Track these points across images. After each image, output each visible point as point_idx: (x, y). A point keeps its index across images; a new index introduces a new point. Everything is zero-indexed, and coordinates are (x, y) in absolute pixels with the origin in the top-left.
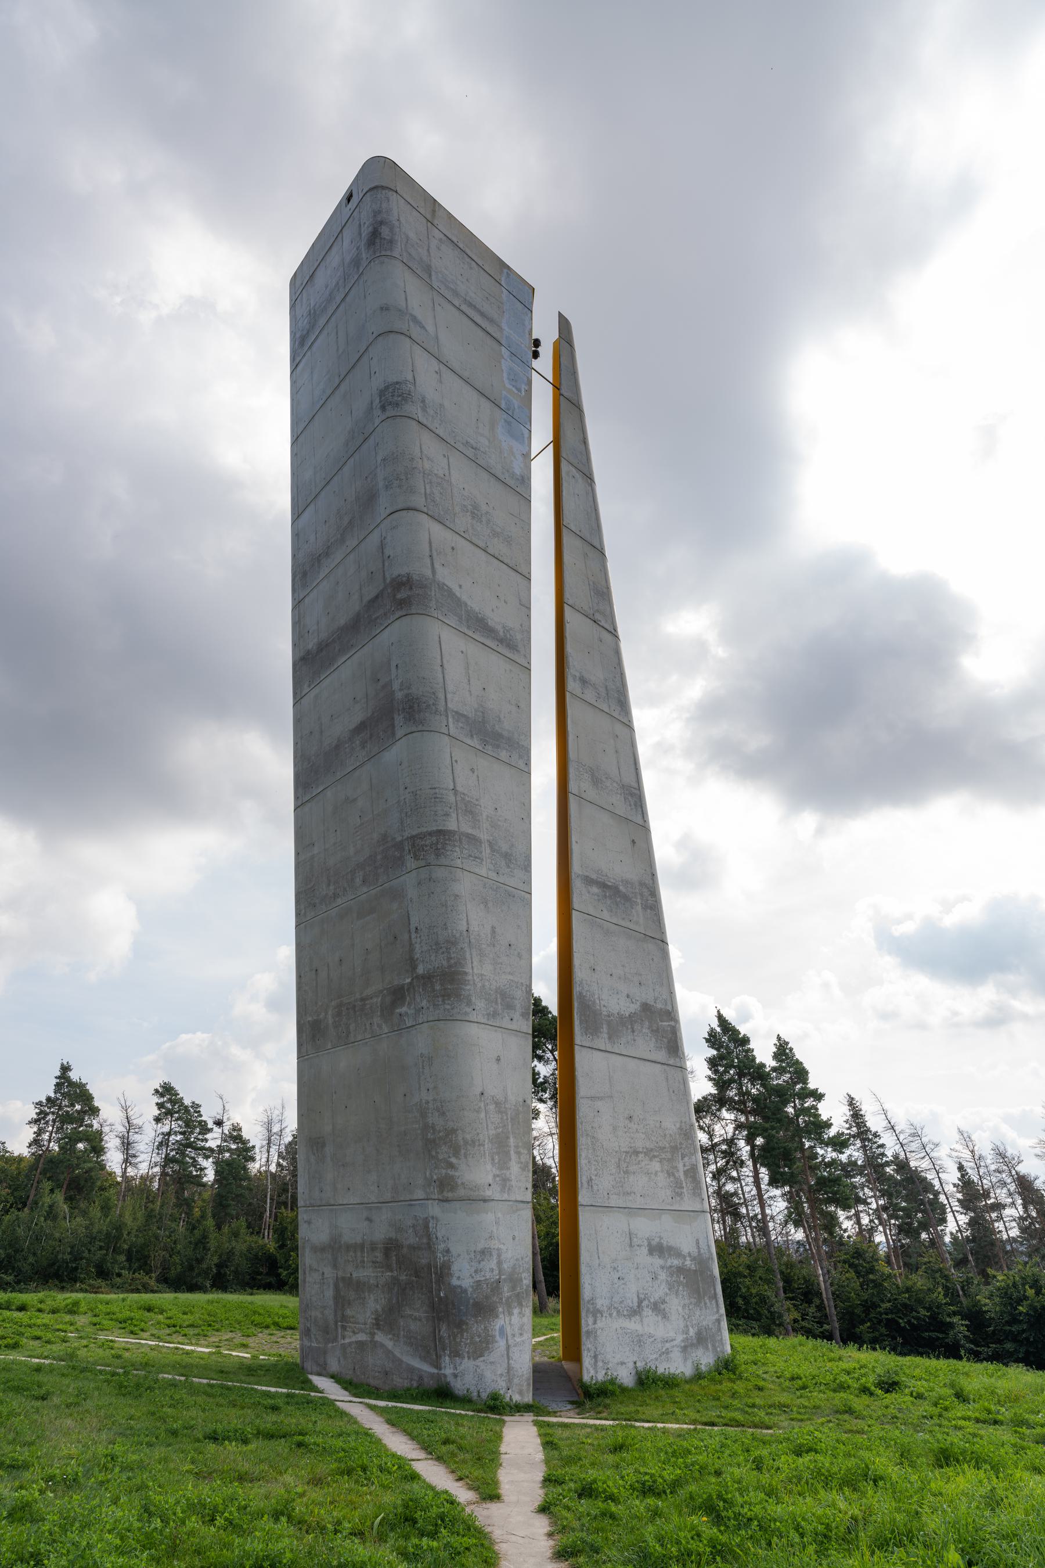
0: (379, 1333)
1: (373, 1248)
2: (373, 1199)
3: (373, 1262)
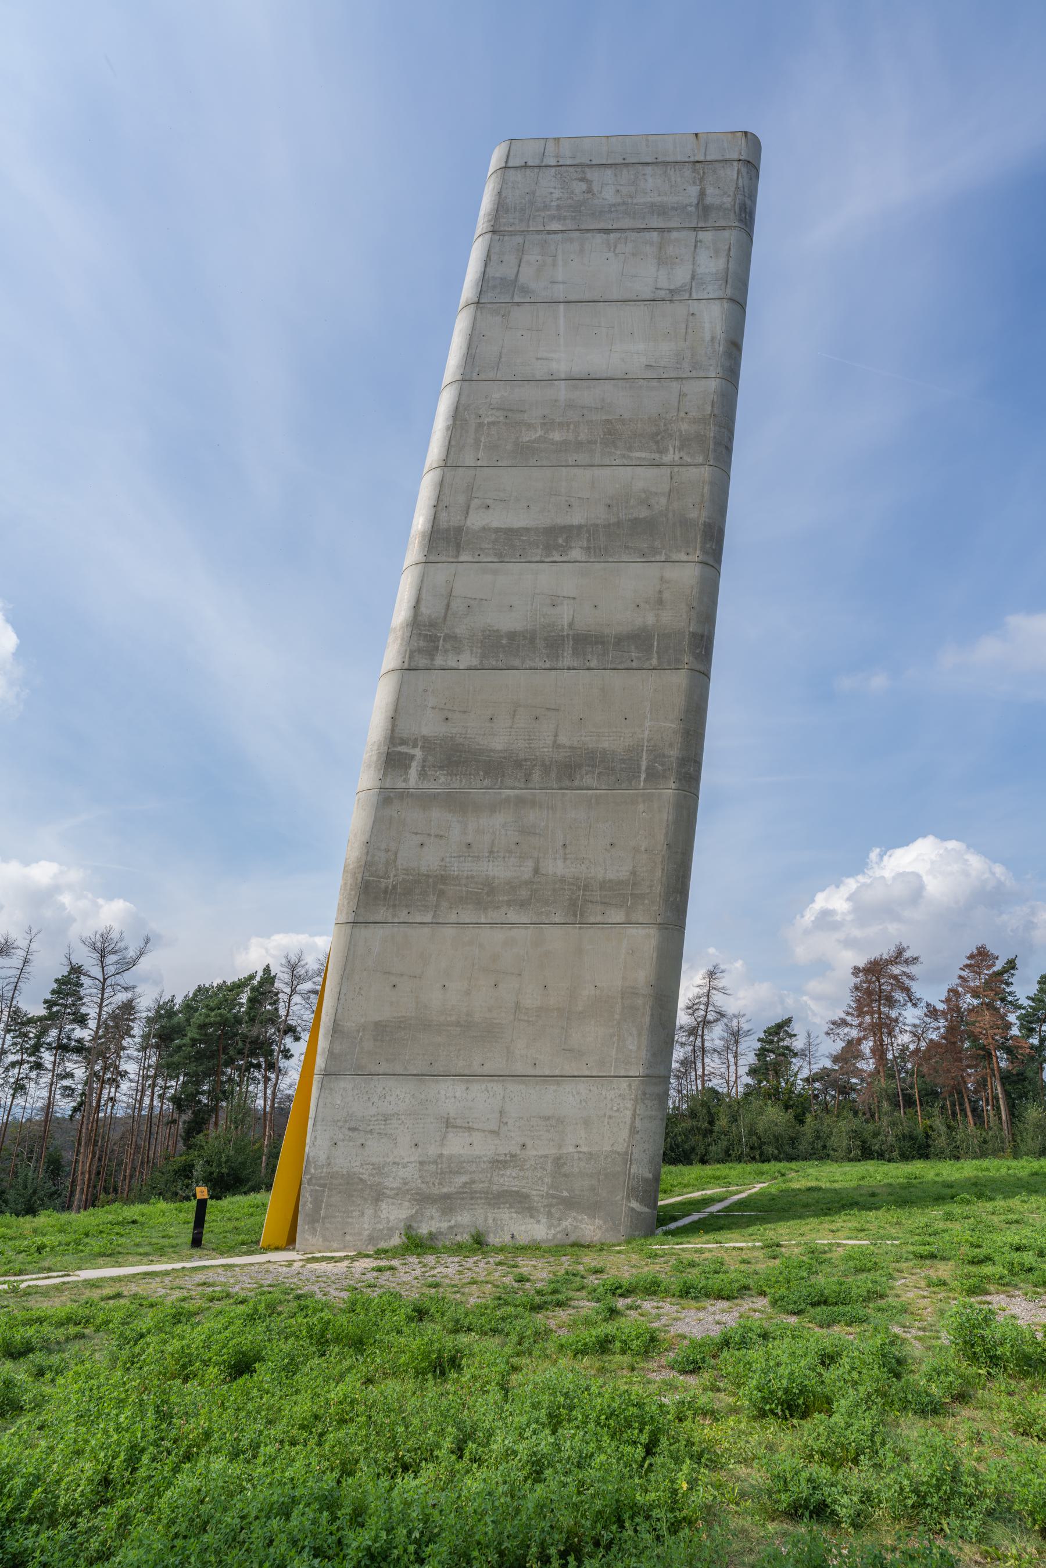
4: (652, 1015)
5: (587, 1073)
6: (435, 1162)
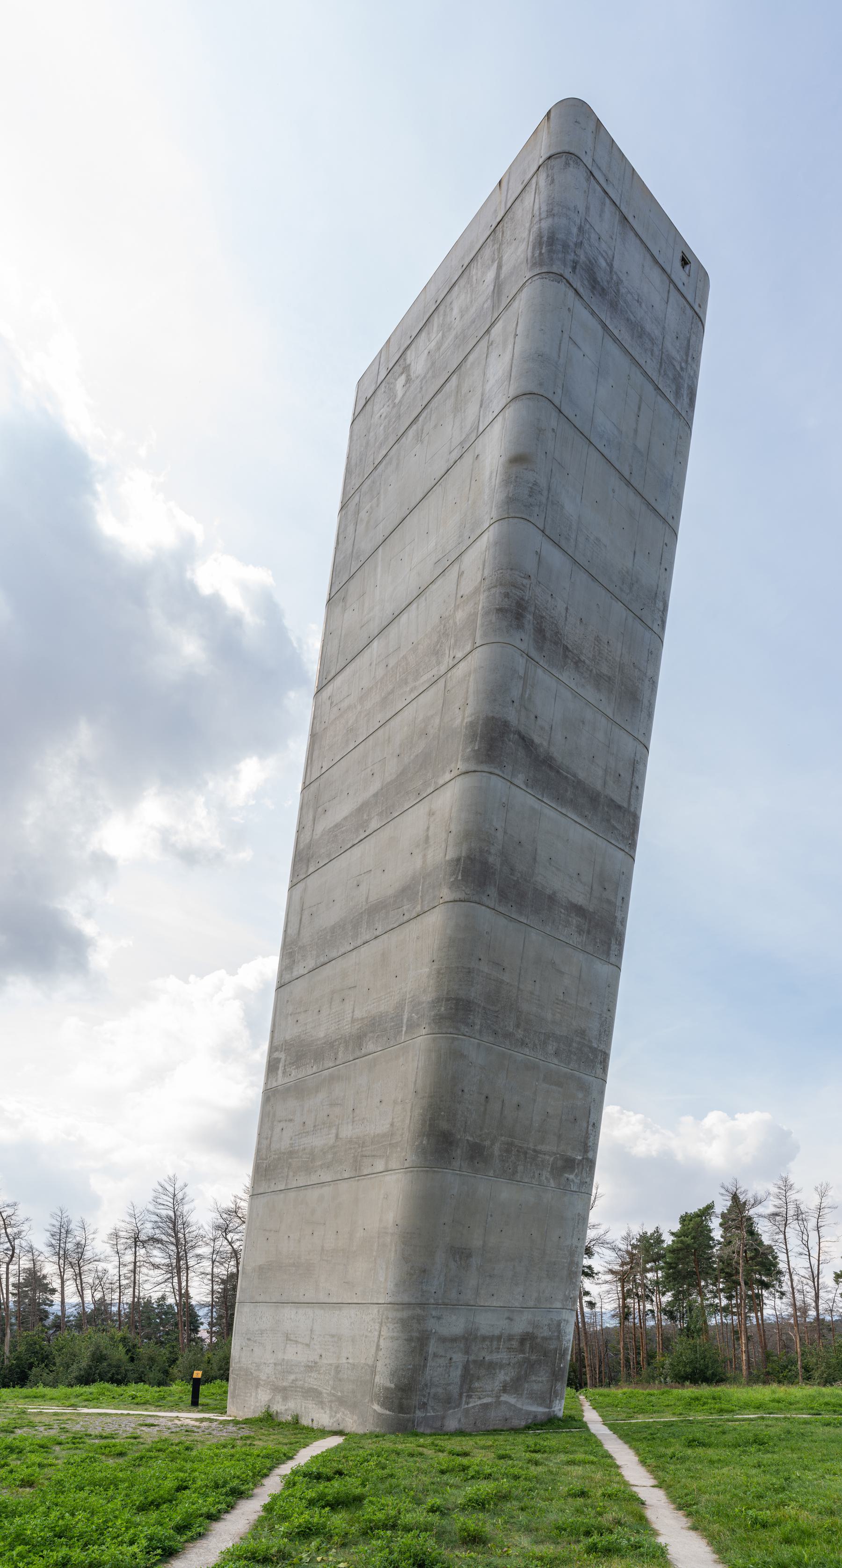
0: (505, 1395)
1: (510, 1338)
2: (517, 1305)
3: (508, 1348)
4: (396, 1251)
5: (355, 1301)
6: (281, 1364)
